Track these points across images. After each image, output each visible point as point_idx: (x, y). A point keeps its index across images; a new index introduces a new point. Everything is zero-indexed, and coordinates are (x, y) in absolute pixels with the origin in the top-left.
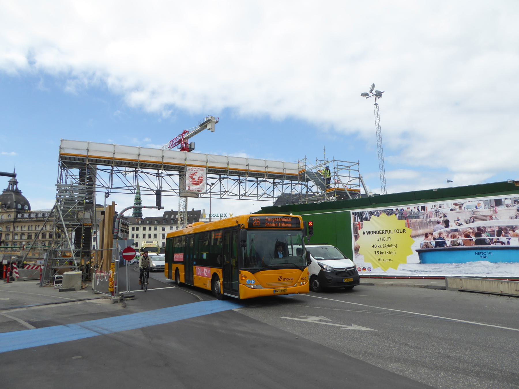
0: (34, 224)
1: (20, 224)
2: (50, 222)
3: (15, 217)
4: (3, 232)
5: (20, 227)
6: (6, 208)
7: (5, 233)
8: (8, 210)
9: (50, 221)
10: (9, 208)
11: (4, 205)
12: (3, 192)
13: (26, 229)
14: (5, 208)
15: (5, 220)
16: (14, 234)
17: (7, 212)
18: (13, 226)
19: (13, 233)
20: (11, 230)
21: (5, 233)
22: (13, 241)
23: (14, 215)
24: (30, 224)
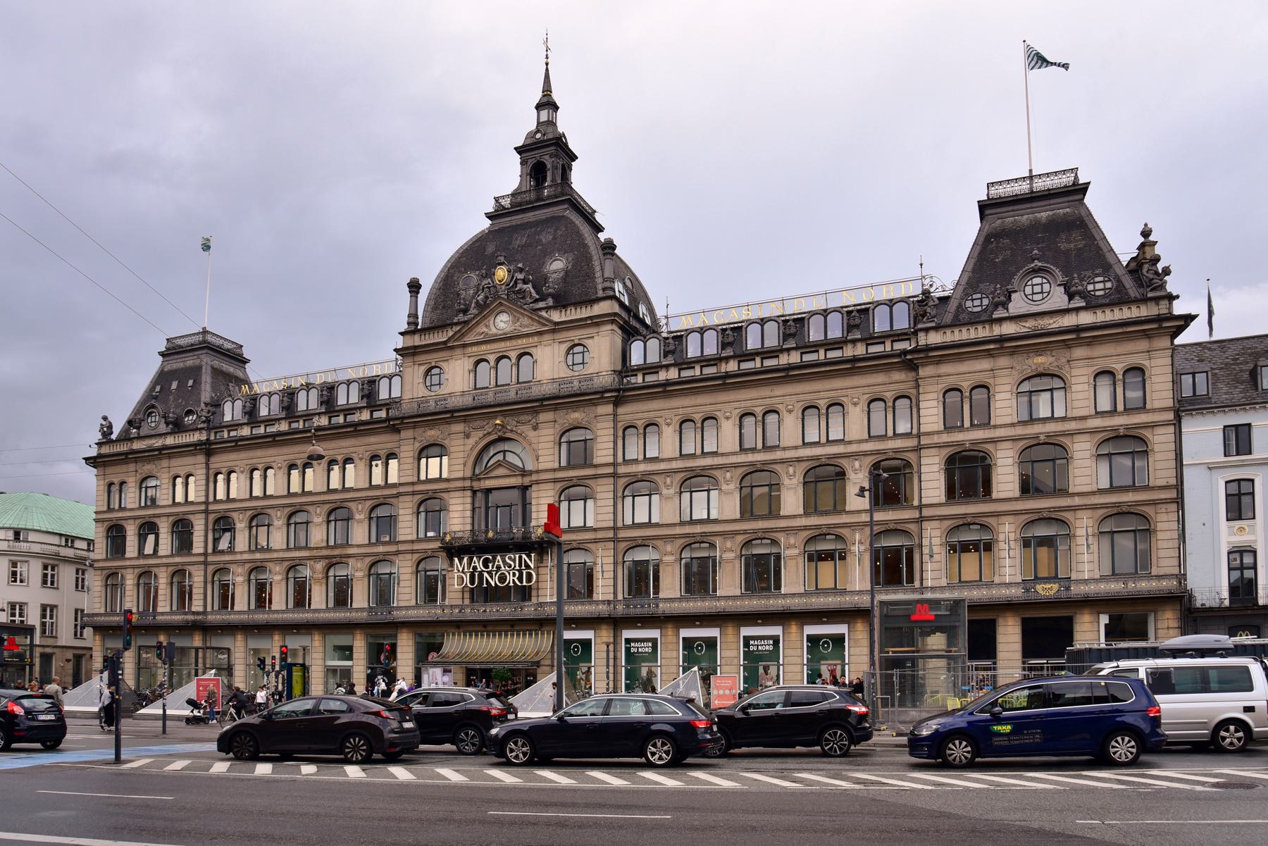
0: (788, 396)
1: (668, 410)
2: (945, 368)
3: (619, 367)
4: (534, 477)
5: (669, 433)
6: (541, 305)
7: (555, 481)
8: (556, 316)
9: (940, 361)
10: (562, 302)
11: (525, 282)
12: (490, 216)
13: (724, 437)
14: (536, 301)
15: (549, 389)
16: (622, 482)
17: (557, 328)
18: (615, 428)
19: (615, 475)
20: (603, 453)
21: (555, 481)
22: (622, 534)
23: (613, 343)
24: (754, 398)
